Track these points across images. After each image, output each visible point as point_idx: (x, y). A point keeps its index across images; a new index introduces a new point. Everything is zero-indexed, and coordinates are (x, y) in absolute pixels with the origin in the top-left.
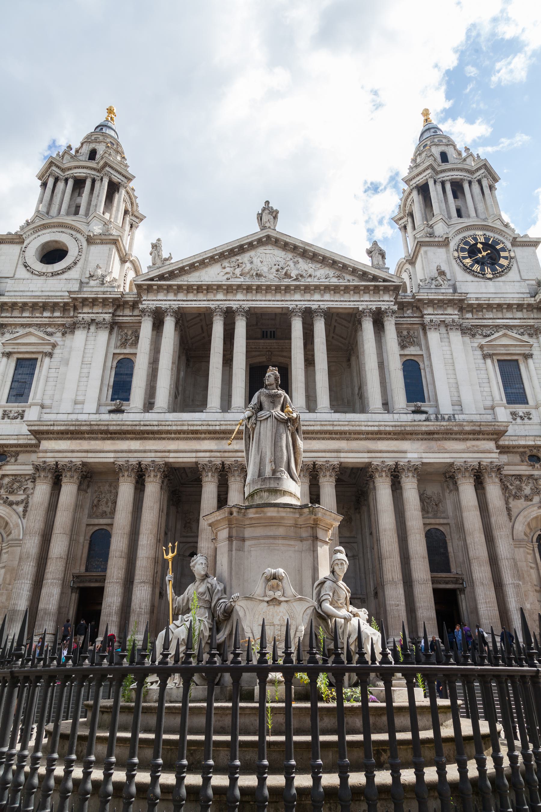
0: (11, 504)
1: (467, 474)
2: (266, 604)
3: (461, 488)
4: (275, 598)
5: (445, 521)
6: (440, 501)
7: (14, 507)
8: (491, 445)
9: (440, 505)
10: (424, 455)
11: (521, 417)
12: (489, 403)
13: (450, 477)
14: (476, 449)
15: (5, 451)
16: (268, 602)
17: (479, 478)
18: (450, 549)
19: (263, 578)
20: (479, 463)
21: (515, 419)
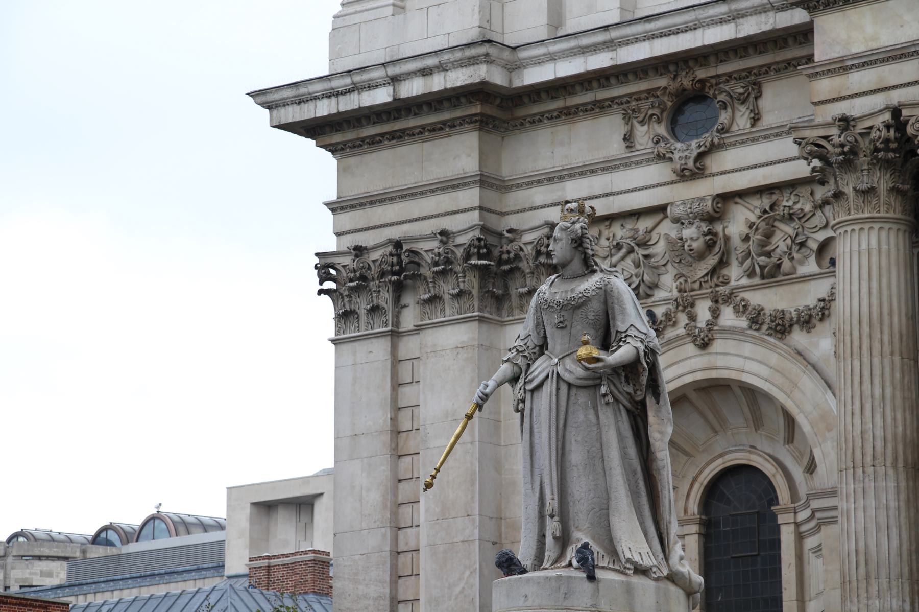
0: (781, 327)
7: (798, 337)
15: (703, 81)
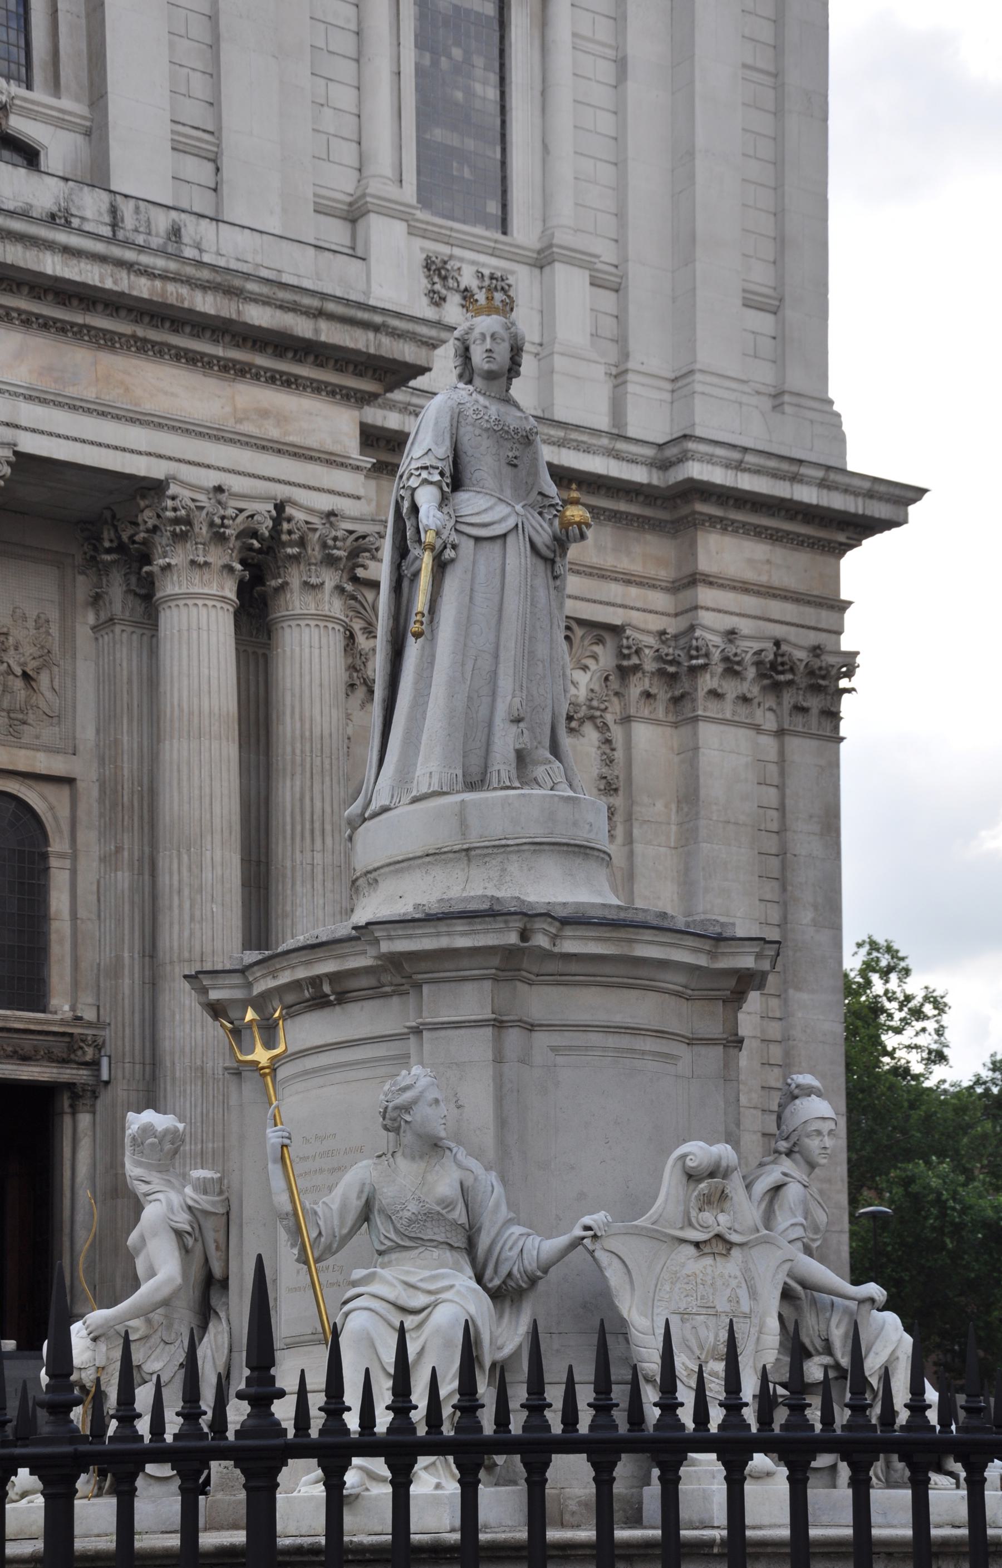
1: (217, 556)
2: (691, 1250)
3: (174, 620)
4: (718, 1236)
5: (57, 766)
6: (46, 659)
8: (336, 426)
9: (44, 680)
10: (29, 413)
11: (467, 295)
12: (342, 184)
13: (121, 548)
14: (273, 432)
16: (697, 1245)
17: (261, 571)
18: (59, 901)
19: (678, 1171)
20: (280, 507)
21: (437, 300)
